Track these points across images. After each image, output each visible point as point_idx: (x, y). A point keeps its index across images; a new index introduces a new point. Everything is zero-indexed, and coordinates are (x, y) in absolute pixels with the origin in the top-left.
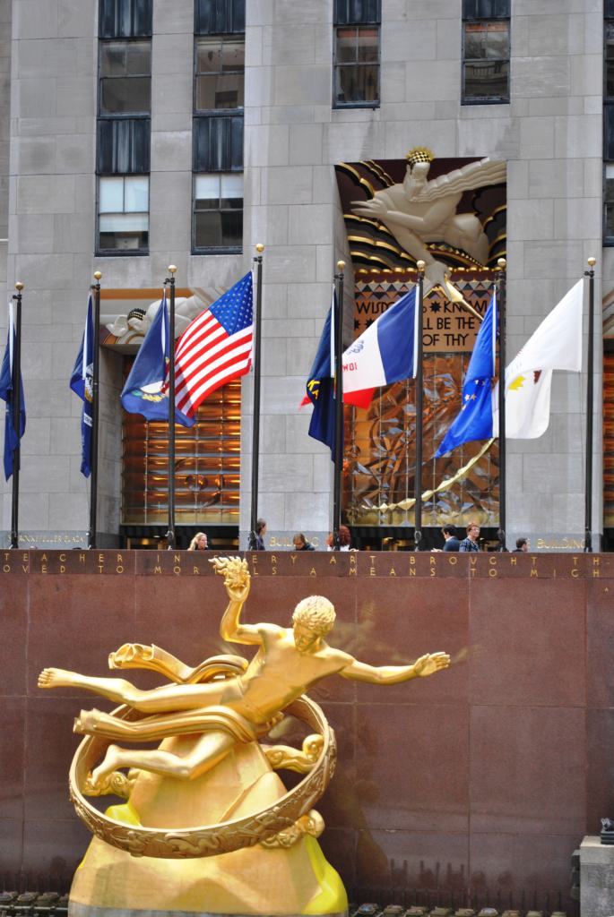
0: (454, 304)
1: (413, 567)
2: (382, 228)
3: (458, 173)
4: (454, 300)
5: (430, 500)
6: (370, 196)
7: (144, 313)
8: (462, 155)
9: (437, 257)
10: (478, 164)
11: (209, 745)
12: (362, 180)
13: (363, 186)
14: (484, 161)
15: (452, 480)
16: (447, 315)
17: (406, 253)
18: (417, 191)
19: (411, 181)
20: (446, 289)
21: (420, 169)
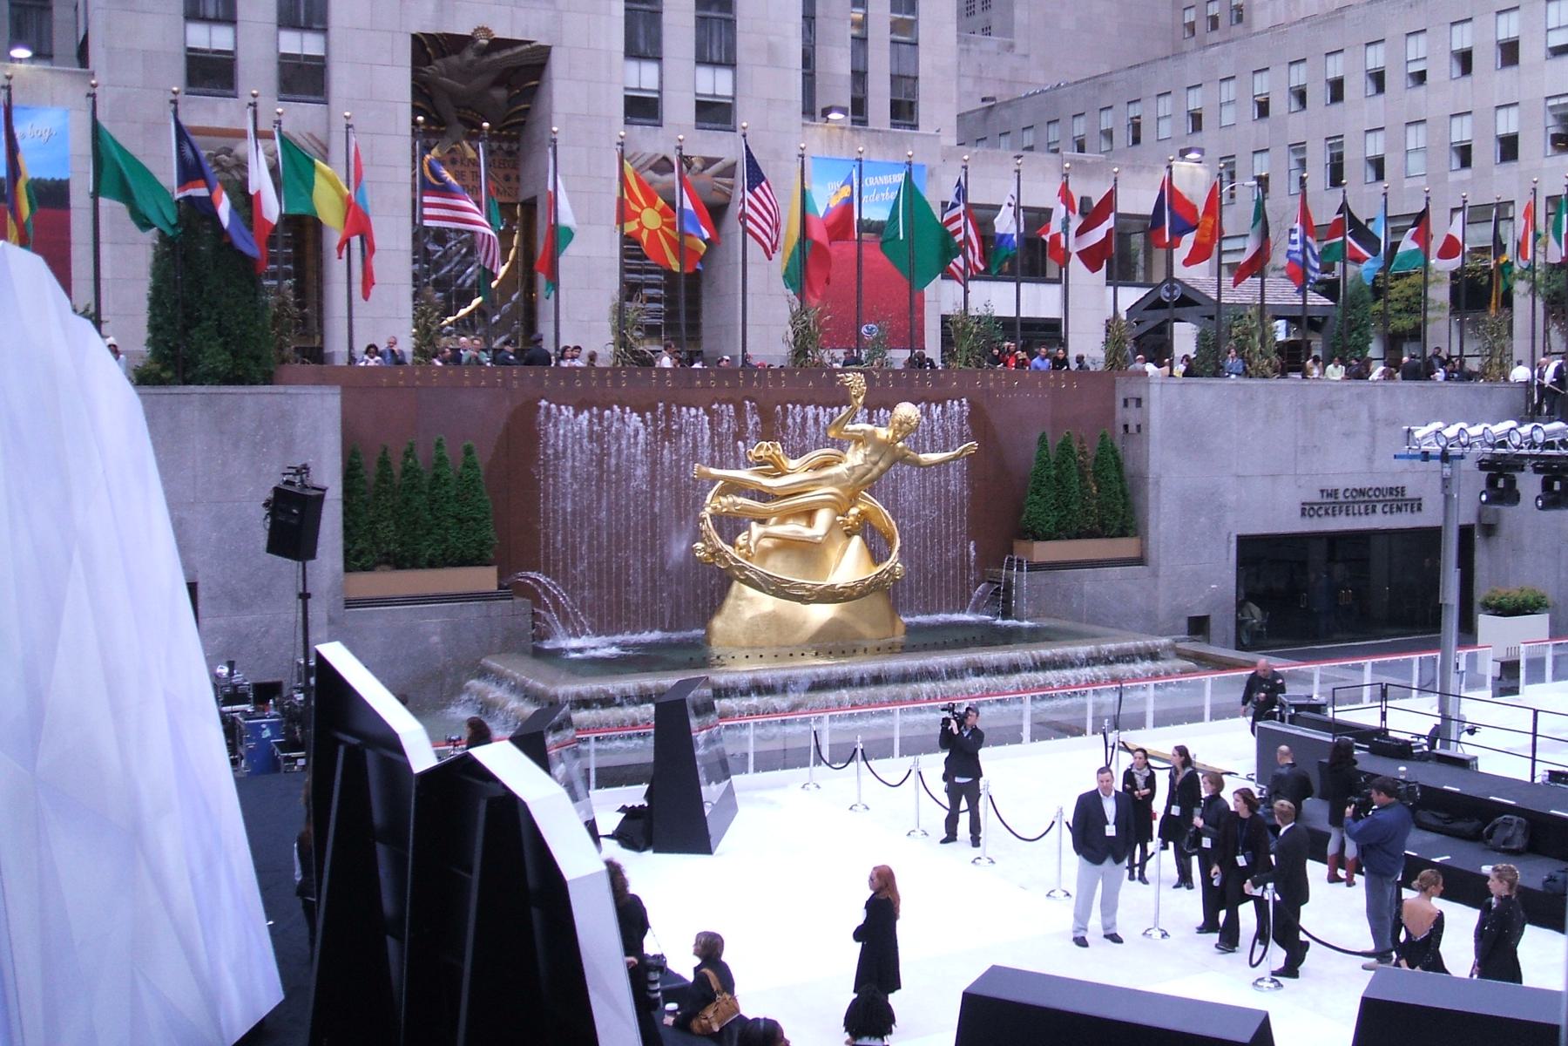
0: (470, 160)
1: (879, 380)
2: (426, 91)
3: (508, 52)
4: (469, 157)
5: (450, 324)
6: (430, 63)
7: (232, 150)
8: (518, 36)
9: (461, 120)
10: (528, 46)
11: (823, 518)
12: (428, 49)
13: (428, 53)
14: (533, 45)
15: (469, 308)
16: (463, 169)
17: (437, 113)
18: (471, 63)
19: (469, 55)
20: (462, 146)
21: (483, 45)
